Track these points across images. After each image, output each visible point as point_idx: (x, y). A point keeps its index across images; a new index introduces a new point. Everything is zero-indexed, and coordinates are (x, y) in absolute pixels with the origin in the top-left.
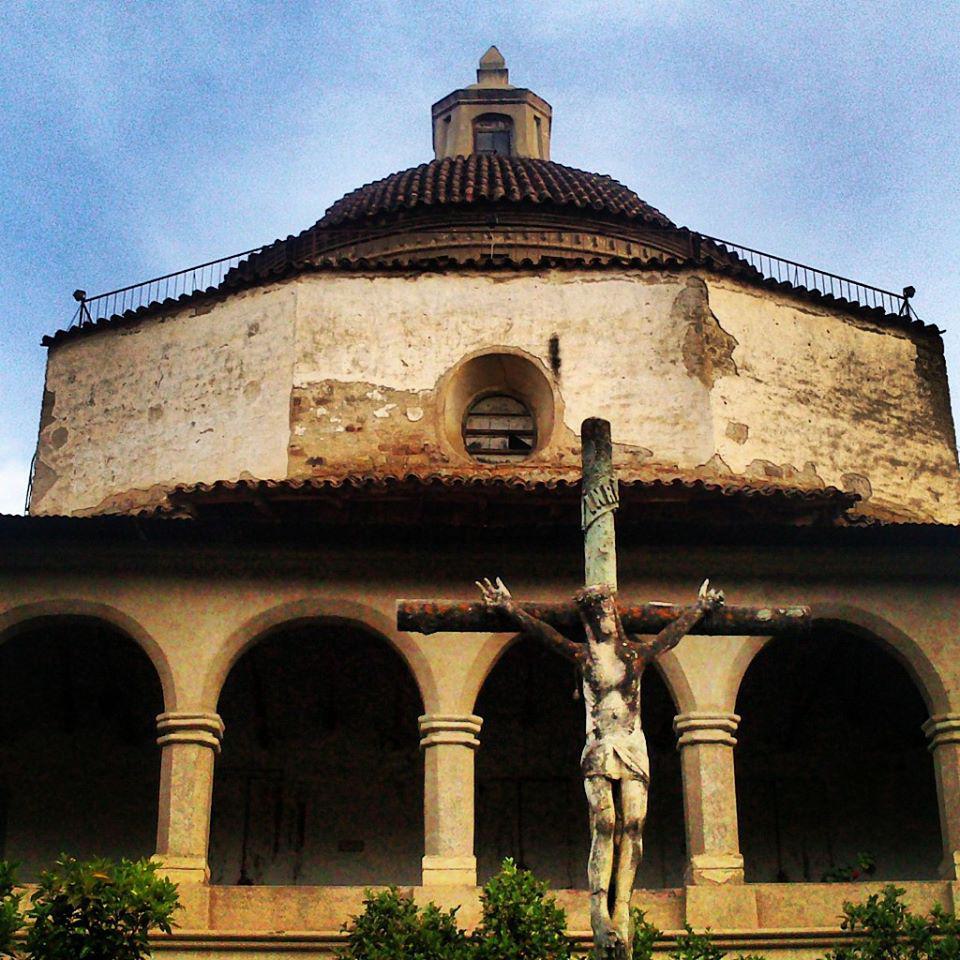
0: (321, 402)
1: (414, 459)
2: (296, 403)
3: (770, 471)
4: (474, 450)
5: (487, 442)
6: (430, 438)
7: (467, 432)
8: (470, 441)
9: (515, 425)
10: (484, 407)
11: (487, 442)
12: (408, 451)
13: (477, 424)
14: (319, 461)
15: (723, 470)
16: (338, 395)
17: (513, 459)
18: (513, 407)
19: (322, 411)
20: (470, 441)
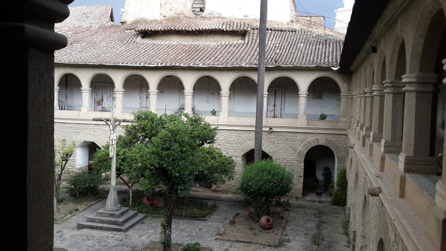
0: (165, 4)
1: (182, 16)
2: (161, 4)
3: (245, 16)
4: (194, 11)
5: (196, 10)
6: (184, 12)
7: (193, 8)
8: (193, 9)
9: (201, 6)
10: (196, 2)
11: (196, 10)
12: (180, 14)
13: (195, 6)
14: (165, 16)
15: (235, 17)
16: (168, 3)
17: (199, 13)
18: (201, 2)
19: (165, 6)
20: (193, 9)
